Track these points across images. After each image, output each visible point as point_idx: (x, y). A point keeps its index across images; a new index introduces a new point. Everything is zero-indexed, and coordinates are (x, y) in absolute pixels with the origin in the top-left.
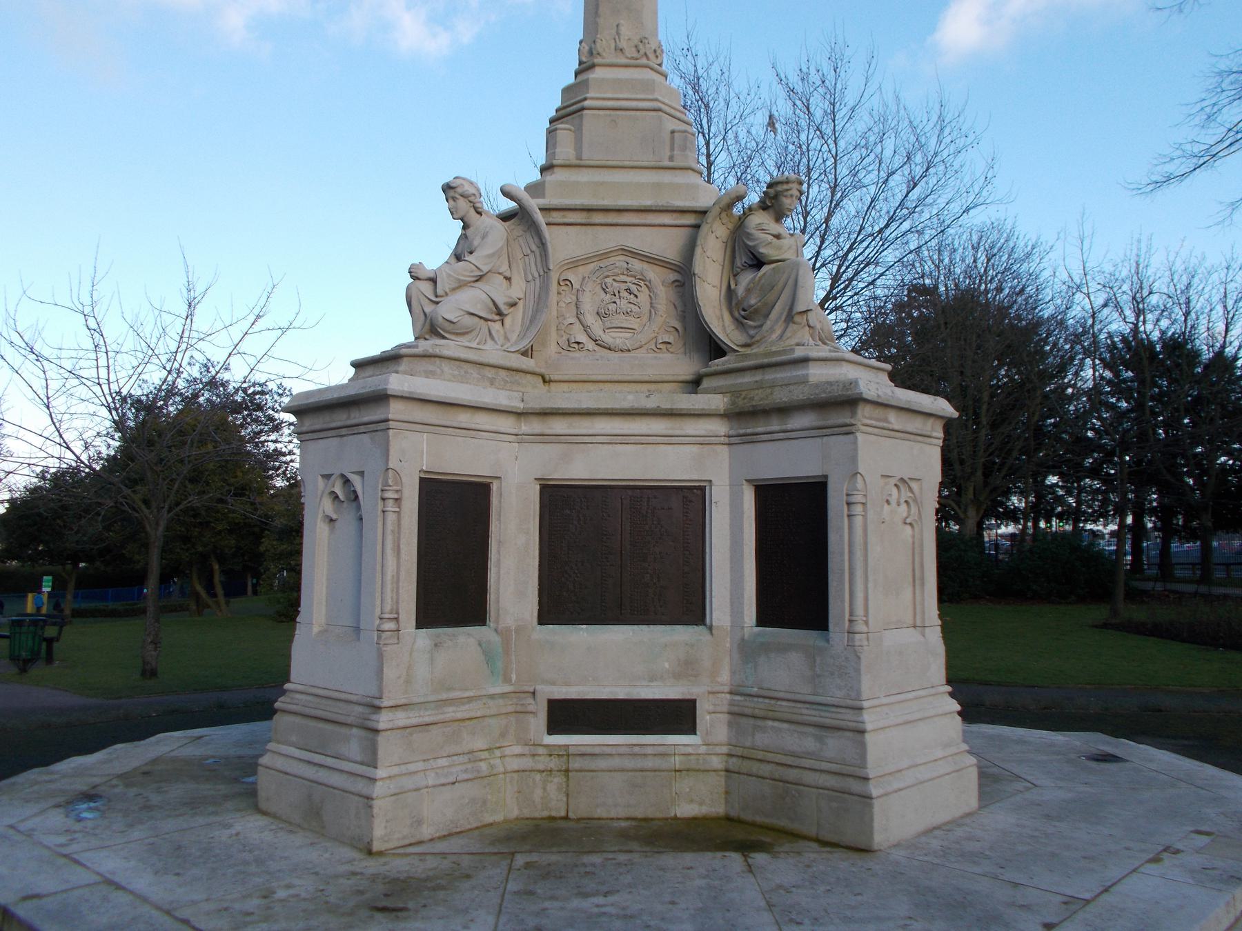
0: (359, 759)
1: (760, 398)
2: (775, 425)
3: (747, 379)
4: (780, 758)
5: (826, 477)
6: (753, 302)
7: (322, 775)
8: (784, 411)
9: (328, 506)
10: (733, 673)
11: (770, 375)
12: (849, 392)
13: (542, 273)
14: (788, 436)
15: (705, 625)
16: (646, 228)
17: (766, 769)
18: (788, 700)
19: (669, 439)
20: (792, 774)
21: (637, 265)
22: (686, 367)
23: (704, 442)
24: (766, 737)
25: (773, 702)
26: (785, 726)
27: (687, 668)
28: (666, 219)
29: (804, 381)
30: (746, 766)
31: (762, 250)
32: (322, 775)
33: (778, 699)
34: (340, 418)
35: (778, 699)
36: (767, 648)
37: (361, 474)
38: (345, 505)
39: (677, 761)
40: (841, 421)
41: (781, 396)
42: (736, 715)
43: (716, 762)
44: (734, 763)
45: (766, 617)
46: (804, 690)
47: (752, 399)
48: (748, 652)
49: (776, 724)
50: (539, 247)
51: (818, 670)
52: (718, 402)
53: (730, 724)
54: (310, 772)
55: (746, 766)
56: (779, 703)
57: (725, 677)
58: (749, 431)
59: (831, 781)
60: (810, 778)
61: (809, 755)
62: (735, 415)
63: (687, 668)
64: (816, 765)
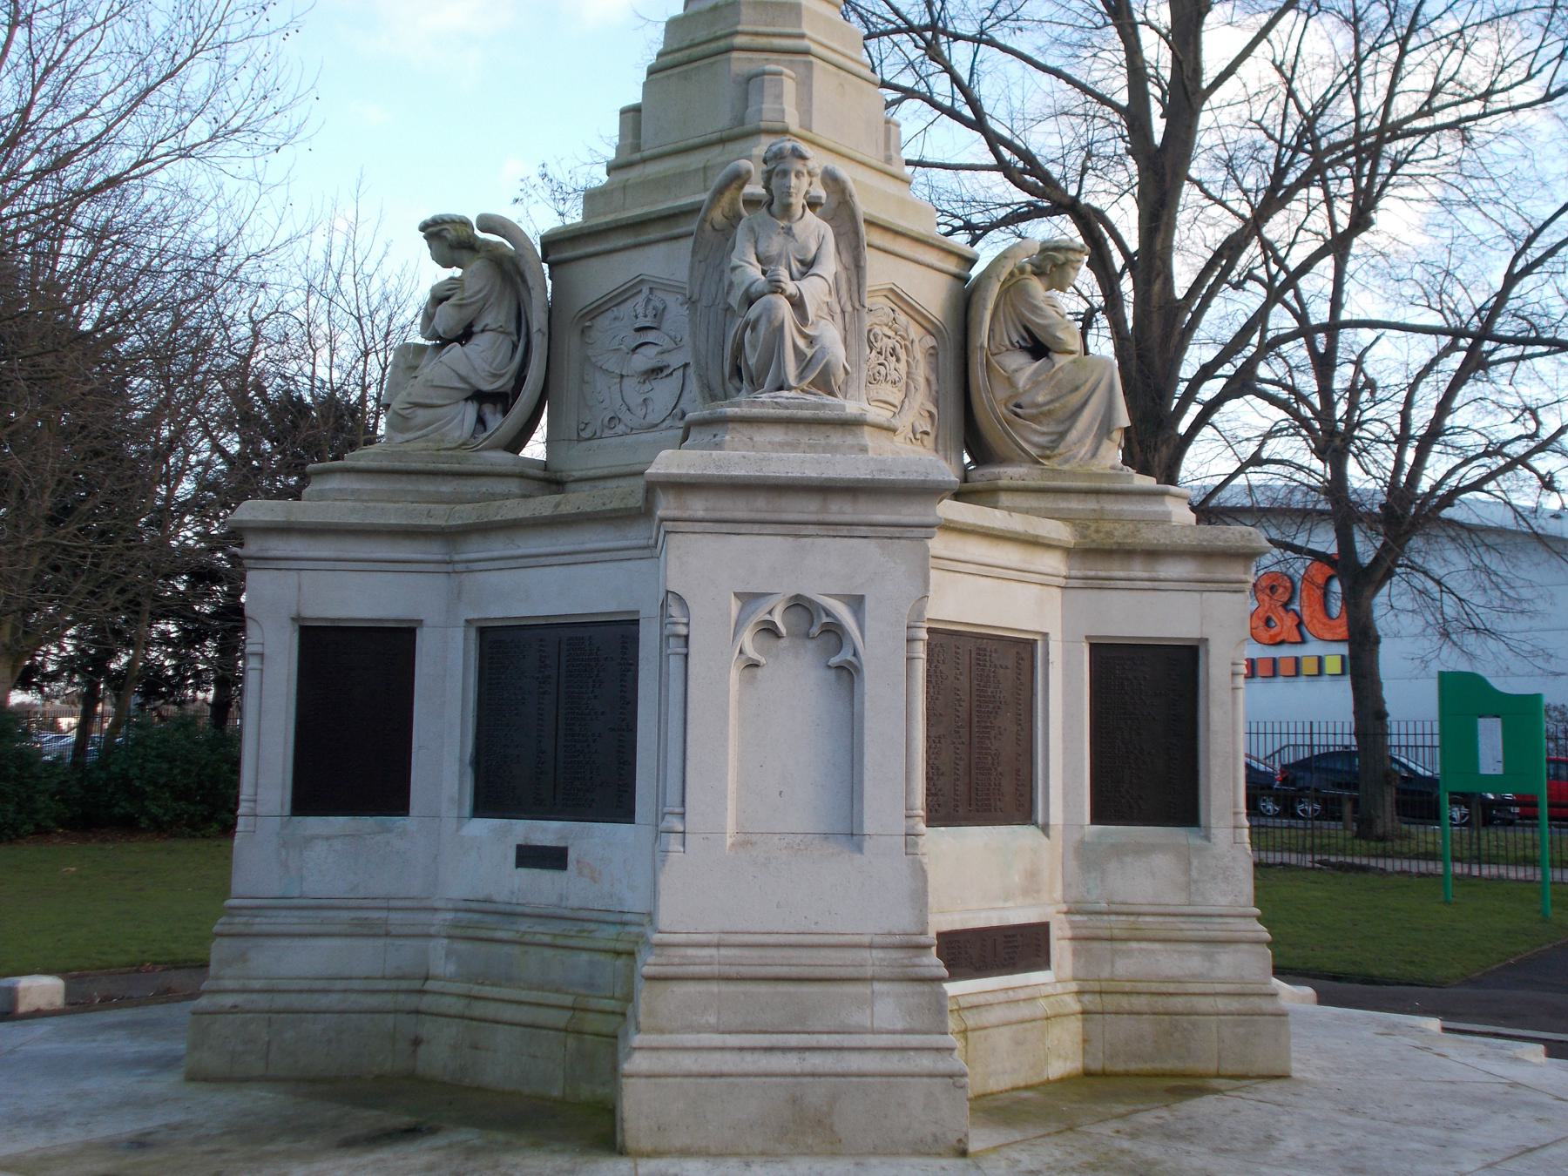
0: (899, 1026)
1: (1120, 533)
2: (1138, 570)
3: (1074, 504)
4: (1155, 987)
5: (1205, 641)
6: (1040, 399)
7: (815, 1062)
8: (1153, 554)
10: (1066, 886)
12: (1254, 545)
13: (849, 308)
14: (1156, 585)
15: (1035, 824)
16: (917, 266)
17: (1140, 1003)
18: (1153, 914)
20: (1178, 1003)
24: (1133, 963)
25: (1132, 918)
26: (1157, 946)
27: (1032, 885)
29: (1164, 519)
30: (1111, 1002)
31: (1059, 334)
32: (815, 1062)
33: (1139, 914)
34: (808, 508)
35: (1139, 914)
36: (1118, 851)
37: (856, 603)
38: (783, 643)
39: (1043, 1007)
40: (1233, 576)
44: (1091, 1001)
45: (1103, 811)
46: (1174, 899)
47: (1110, 534)
48: (1086, 857)
49: (1144, 945)
50: (846, 269)
51: (1194, 874)
52: (1059, 531)
53: (1076, 953)
54: (791, 1062)
55: (1111, 1002)
56: (1141, 919)
58: (1102, 574)
59: (1235, 1004)
60: (1204, 1004)
61: (1196, 978)
62: (1079, 553)
64: (1209, 988)
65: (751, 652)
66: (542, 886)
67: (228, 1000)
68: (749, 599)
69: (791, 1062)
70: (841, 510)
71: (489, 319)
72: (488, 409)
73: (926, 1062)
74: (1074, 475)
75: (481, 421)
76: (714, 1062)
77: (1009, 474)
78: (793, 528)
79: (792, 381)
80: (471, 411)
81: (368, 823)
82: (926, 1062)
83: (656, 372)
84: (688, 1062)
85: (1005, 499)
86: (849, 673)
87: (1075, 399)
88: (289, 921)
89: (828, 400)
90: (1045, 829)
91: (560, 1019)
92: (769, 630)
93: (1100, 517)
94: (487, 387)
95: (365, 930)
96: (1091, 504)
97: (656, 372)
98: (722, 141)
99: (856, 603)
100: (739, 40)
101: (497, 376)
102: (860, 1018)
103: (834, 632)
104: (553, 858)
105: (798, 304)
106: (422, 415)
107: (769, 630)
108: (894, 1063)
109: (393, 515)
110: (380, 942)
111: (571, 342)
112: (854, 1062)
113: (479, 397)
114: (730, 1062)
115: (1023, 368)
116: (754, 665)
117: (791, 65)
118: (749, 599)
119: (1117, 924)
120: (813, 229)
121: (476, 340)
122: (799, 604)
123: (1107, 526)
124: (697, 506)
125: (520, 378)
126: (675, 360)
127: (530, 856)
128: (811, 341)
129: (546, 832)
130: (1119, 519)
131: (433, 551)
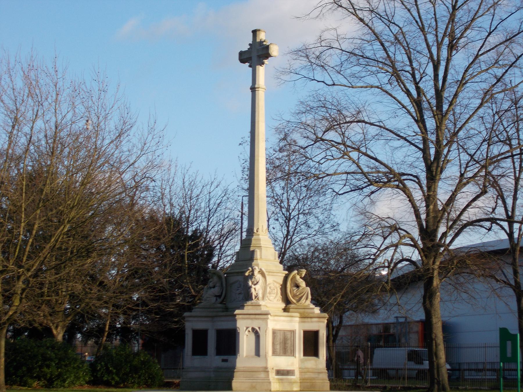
1: (306, 315)
2: (309, 320)
9: (247, 332)
14: (312, 322)
17: (308, 381)
20: (314, 381)
21: (275, 284)
22: (283, 305)
29: (314, 313)
30: (304, 381)
32: (254, 381)
37: (259, 328)
41: (311, 315)
42: (301, 373)
43: (299, 381)
44: (301, 381)
46: (314, 367)
48: (302, 361)
55: (304, 381)
57: (297, 366)
59: (322, 381)
62: (301, 317)
66: (225, 364)
70: (257, 316)
71: (218, 285)
73: (267, 381)
75: (216, 300)
76: (243, 381)
78: (252, 319)
80: (215, 298)
81: (202, 357)
82: (267, 381)
83: (240, 293)
84: (240, 381)
87: (302, 295)
92: (249, 331)
96: (303, 310)
97: (240, 293)
106: (208, 299)
107: (249, 331)
108: (263, 381)
112: (259, 381)
113: (216, 296)
114: (245, 381)
118: (247, 328)
122: (253, 329)
125: (222, 293)
129: (225, 357)
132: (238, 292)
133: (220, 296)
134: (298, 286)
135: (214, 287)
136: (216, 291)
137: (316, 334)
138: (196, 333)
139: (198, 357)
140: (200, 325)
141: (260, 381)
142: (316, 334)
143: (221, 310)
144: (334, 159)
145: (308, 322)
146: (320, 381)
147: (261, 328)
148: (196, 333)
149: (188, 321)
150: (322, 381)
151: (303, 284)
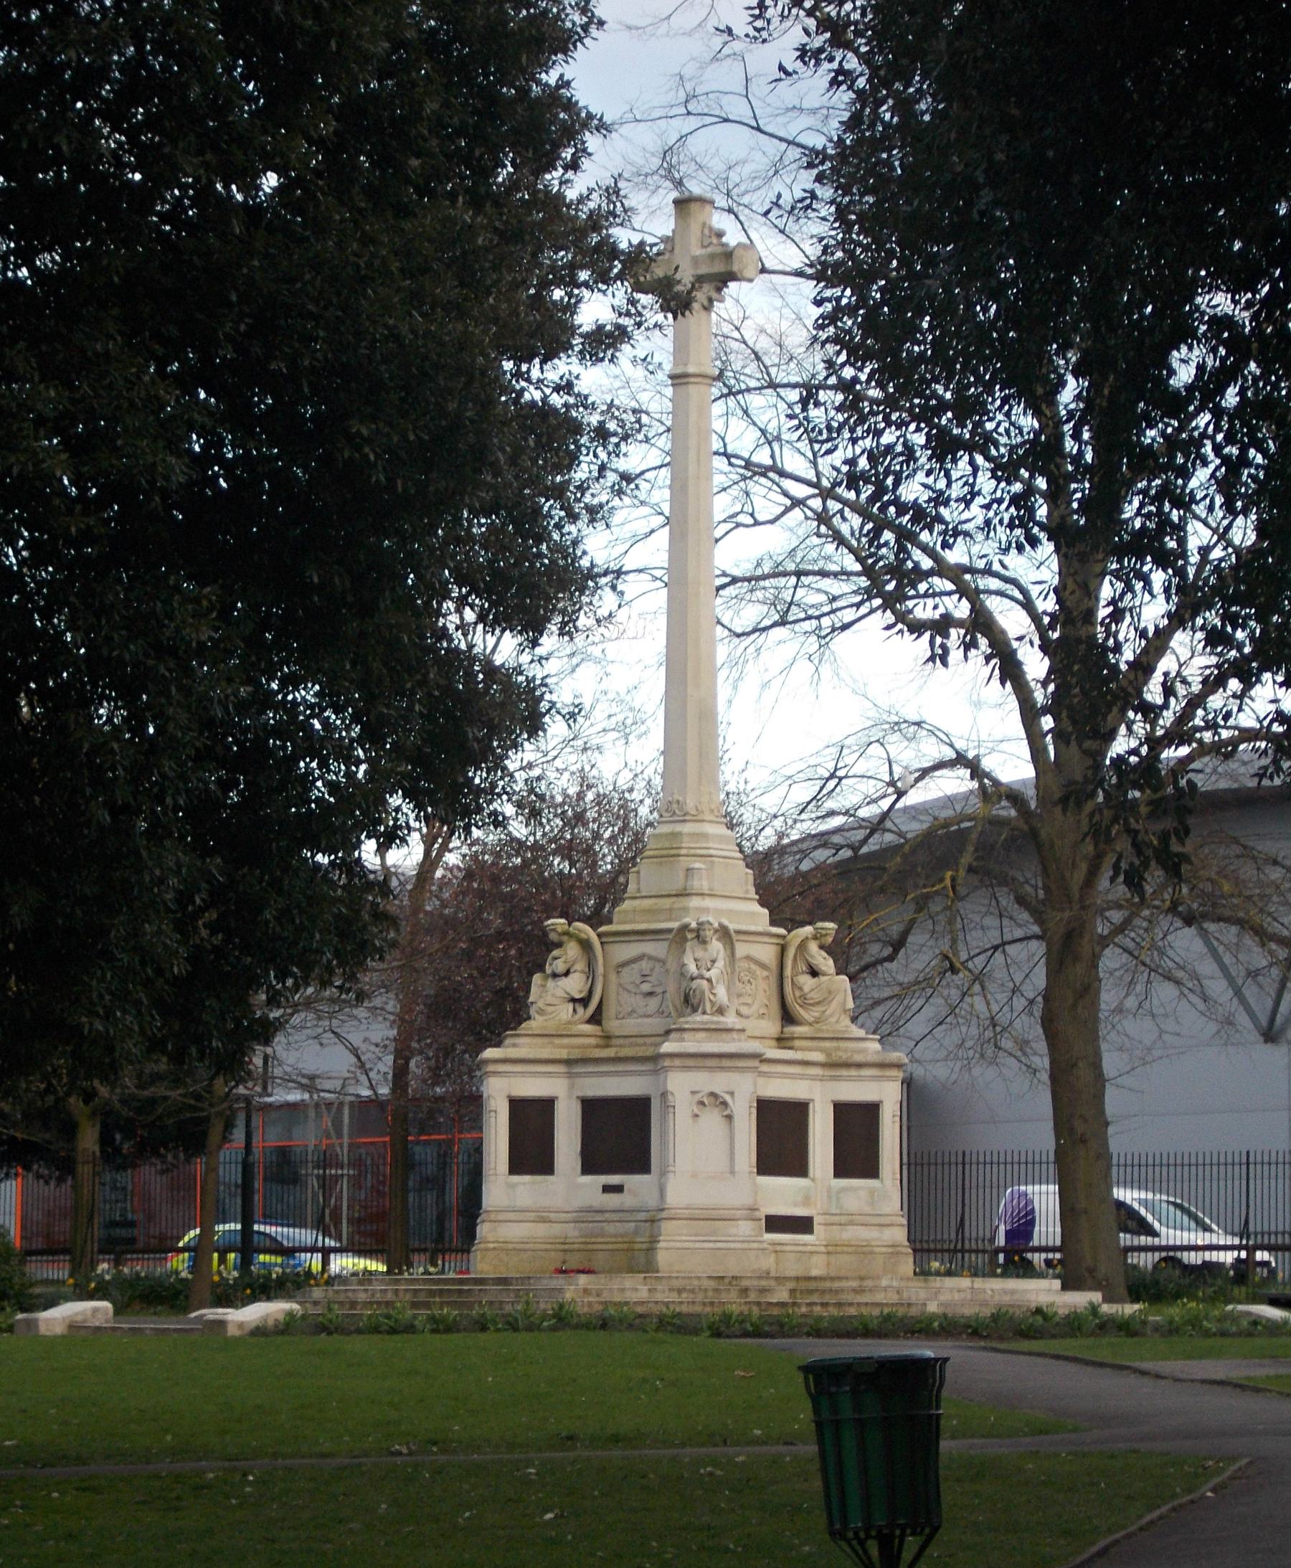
1: (844, 1057)
2: (853, 1072)
3: (827, 1044)
7: (719, 1245)
8: (859, 1066)
11: (843, 1044)
19: (802, 1077)
23: (813, 1078)
24: (850, 1234)
28: (766, 939)
32: (719, 1245)
37: (732, 1094)
41: (858, 1058)
54: (712, 1245)
59: (890, 1250)
60: (878, 1250)
63: (807, 1201)
65: (696, 1111)
66: (613, 1200)
67: (491, 1246)
68: (693, 1093)
69: (712, 1245)
70: (726, 1063)
72: (577, 1005)
73: (755, 1245)
74: (828, 1031)
75: (574, 1010)
77: (798, 1030)
78: (711, 1069)
79: (708, 1011)
80: (571, 1006)
82: (755, 1245)
83: (651, 994)
84: (678, 1245)
85: (797, 1043)
86: (729, 1118)
88: (511, 1216)
89: (721, 1019)
90: (813, 1180)
91: (625, 1246)
93: (838, 1049)
94: (577, 996)
95: (544, 1220)
96: (834, 1044)
97: (651, 994)
98: (676, 895)
99: (732, 1094)
100: (683, 852)
101: (581, 992)
102: (733, 1231)
103: (725, 1104)
104: (618, 1189)
105: (709, 980)
106: (550, 1009)
107: (702, 1103)
108: (746, 1245)
109: (546, 1053)
110: (547, 1225)
111: (613, 977)
112: (732, 1245)
113: (573, 1000)
114: (691, 1245)
115: (807, 982)
116: (697, 1116)
117: (705, 863)
119: (844, 1219)
120: (716, 946)
121: (571, 976)
122: (713, 1095)
123: (840, 1054)
124: (677, 1062)
126: (659, 990)
127: (607, 1189)
128: (714, 995)
129: (614, 1179)
130: (846, 1051)
131: (562, 1068)
132: (646, 987)
133: (585, 1002)
134: (814, 973)
135: (567, 974)
136: (575, 984)
137: (871, 1111)
138: (518, 1106)
139: (527, 1178)
140: (532, 1087)
141: (738, 1245)
142: (871, 1111)
143: (593, 1041)
144: (757, 523)
145: (850, 1079)
146: (884, 1250)
147: (736, 1094)
148: (518, 1106)
149: (495, 1073)
150: (890, 1250)
151: (826, 963)
